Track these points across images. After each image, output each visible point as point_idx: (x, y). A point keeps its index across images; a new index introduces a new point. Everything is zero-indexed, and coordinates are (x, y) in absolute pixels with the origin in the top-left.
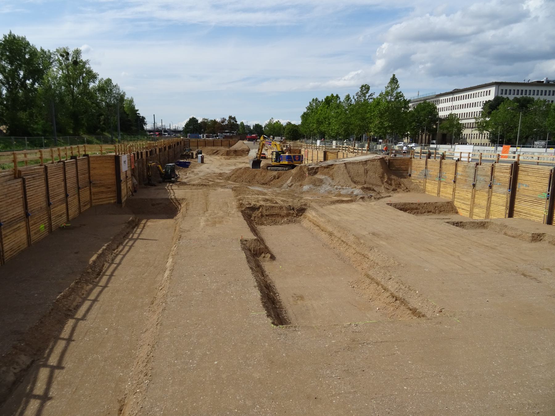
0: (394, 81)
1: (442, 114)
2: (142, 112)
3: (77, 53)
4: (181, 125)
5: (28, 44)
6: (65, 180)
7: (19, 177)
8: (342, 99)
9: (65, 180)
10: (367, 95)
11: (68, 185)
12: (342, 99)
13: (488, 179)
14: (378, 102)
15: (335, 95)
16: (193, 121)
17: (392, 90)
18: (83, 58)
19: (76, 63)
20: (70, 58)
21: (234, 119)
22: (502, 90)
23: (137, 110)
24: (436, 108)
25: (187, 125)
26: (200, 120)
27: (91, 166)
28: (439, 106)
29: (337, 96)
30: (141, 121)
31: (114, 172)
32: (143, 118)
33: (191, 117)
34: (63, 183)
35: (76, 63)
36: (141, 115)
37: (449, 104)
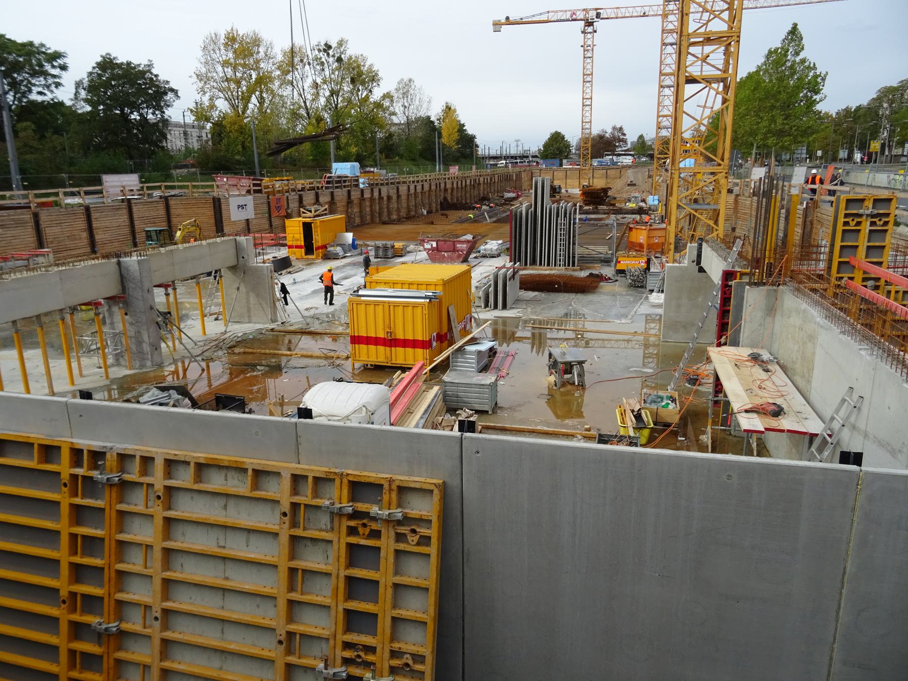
2: (470, 130)
4: (535, 143)
6: (90, 229)
9: (90, 229)
11: (97, 237)
21: (621, 129)
25: (546, 146)
26: (573, 136)
27: (173, 211)
30: (467, 142)
31: (213, 221)
33: (553, 131)
34: (85, 235)
35: (339, 60)
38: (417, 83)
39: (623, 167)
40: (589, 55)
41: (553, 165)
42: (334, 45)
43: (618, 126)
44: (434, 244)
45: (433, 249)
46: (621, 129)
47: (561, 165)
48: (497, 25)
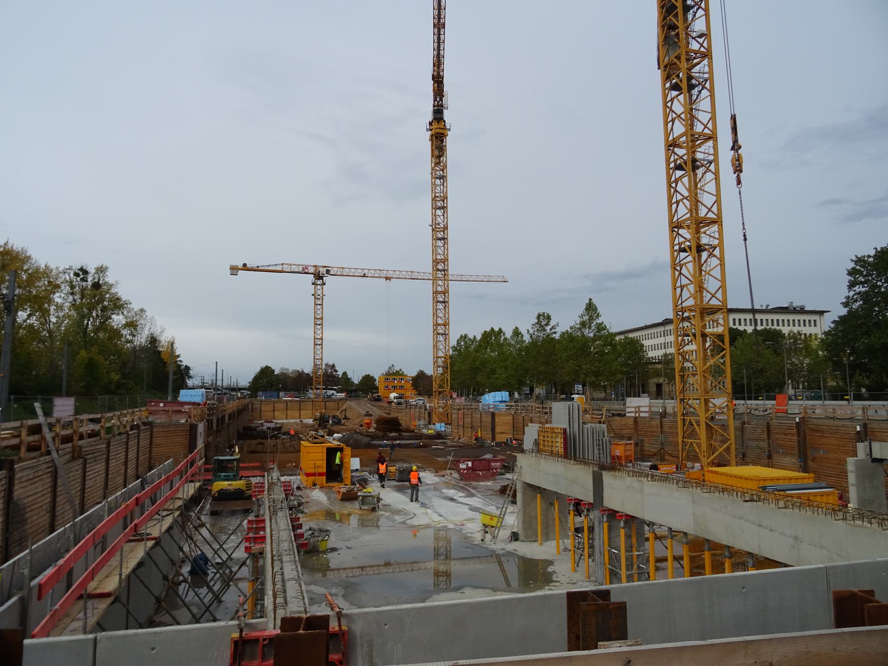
0: (591, 307)
1: (651, 354)
3: (101, 270)
5: (29, 258)
7: (80, 457)
8: (508, 334)
10: (548, 328)
12: (508, 334)
13: (764, 445)
14: (569, 337)
15: (496, 329)
16: (266, 372)
17: (591, 319)
18: (110, 278)
19: (97, 286)
20: (90, 279)
21: (333, 366)
22: (734, 320)
23: (178, 356)
24: (642, 345)
25: (257, 379)
27: (154, 440)
28: (646, 343)
29: (500, 330)
32: (187, 368)
33: (264, 365)
35: (97, 286)
36: (184, 364)
37: (661, 340)
38: (149, 314)
39: (341, 399)
40: (319, 302)
41: (271, 397)
42: (92, 270)
43: (331, 363)
44: (470, 464)
45: (468, 468)
46: (333, 366)
47: (278, 397)
48: (234, 270)
